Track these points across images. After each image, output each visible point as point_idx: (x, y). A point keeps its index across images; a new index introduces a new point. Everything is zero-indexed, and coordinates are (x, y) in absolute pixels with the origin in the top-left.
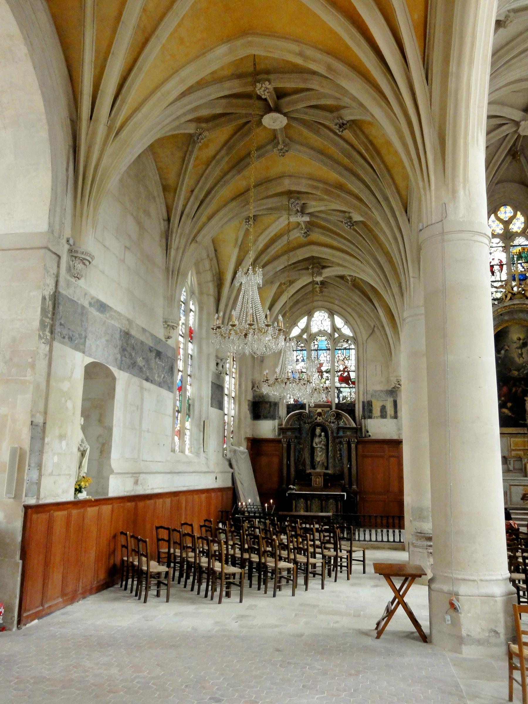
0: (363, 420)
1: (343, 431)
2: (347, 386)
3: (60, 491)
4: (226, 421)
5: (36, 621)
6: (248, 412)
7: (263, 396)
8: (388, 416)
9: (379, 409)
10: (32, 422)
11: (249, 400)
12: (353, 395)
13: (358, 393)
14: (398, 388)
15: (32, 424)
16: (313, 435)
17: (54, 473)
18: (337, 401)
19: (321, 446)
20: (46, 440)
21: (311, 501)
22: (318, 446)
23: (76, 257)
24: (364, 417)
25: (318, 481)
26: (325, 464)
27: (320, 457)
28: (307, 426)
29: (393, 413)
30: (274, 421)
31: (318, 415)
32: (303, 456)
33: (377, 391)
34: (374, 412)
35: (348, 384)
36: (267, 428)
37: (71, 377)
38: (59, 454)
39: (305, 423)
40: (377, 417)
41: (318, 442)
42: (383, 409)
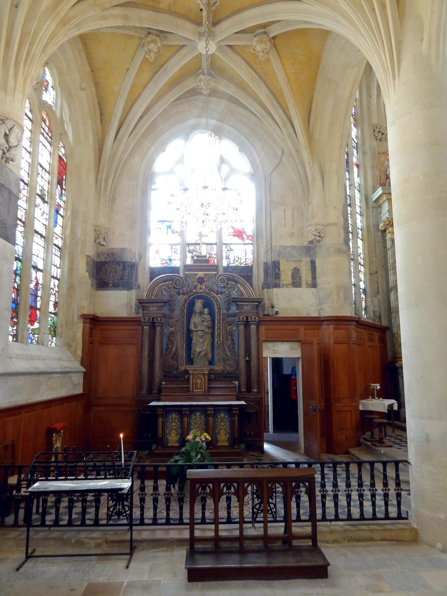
0: (265, 290)
1: (238, 306)
2: (240, 241)
4: (40, 282)
6: (87, 274)
7: (113, 254)
8: (304, 283)
9: (290, 273)
11: (88, 256)
12: (250, 256)
13: (257, 253)
14: (319, 241)
16: (190, 312)
18: (225, 264)
19: (203, 328)
21: (189, 416)
22: (199, 328)
24: (267, 285)
25: (199, 383)
26: (210, 356)
27: (201, 346)
28: (182, 298)
29: (310, 279)
30: (129, 292)
31: (198, 282)
32: (175, 344)
33: (287, 247)
34: (282, 277)
35: (242, 238)
36: (117, 303)
39: (179, 294)
40: (287, 286)
41: (199, 322)
42: (296, 273)
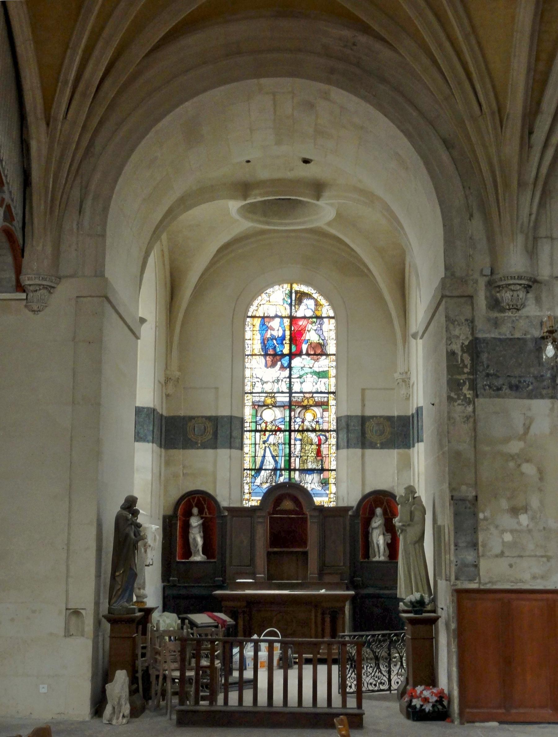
3: (527, 576)
5: (495, 724)
10: (452, 497)
15: (452, 499)
17: (507, 554)
20: (481, 516)
23: (499, 287)
37: (526, 433)
38: (512, 531)
